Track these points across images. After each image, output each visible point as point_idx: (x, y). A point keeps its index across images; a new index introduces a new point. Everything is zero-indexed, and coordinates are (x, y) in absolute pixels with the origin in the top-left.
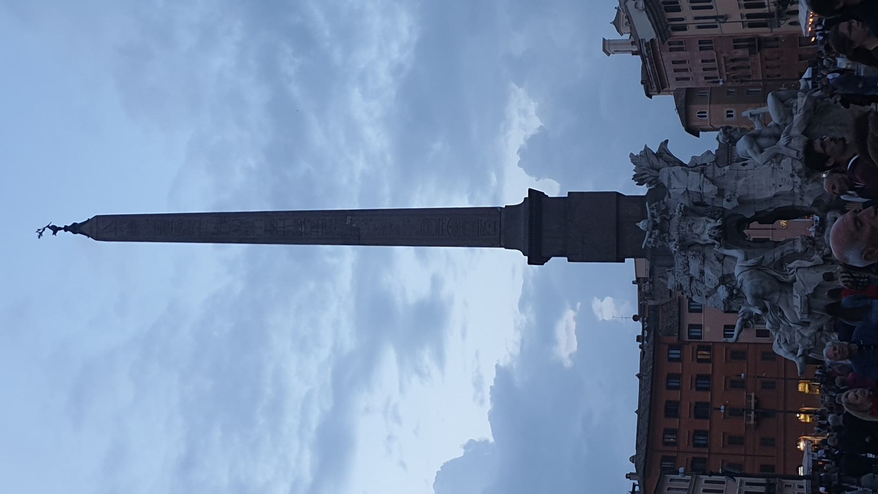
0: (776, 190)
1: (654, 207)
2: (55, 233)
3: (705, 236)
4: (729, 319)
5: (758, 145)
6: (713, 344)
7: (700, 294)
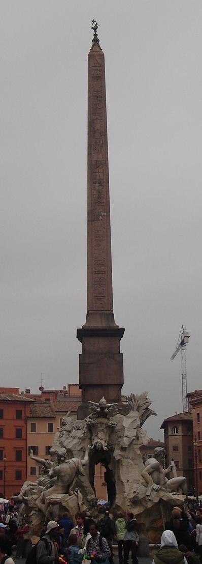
2: (93, 28)
4: (42, 451)
5: (153, 472)
6: (24, 439)
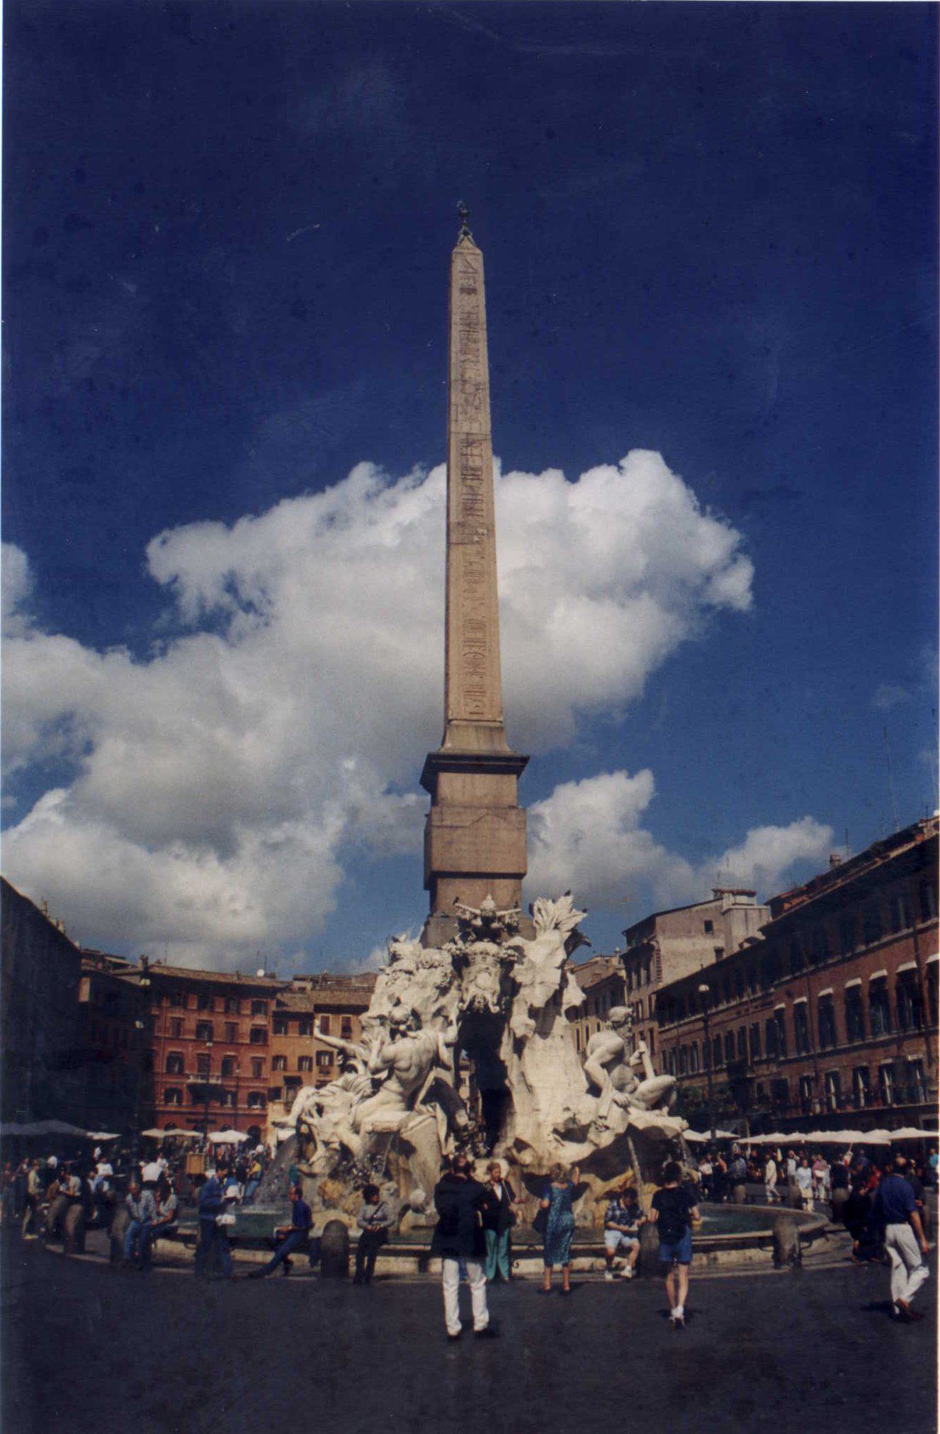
1: (513, 920)
3: (473, 990)
7: (389, 984)
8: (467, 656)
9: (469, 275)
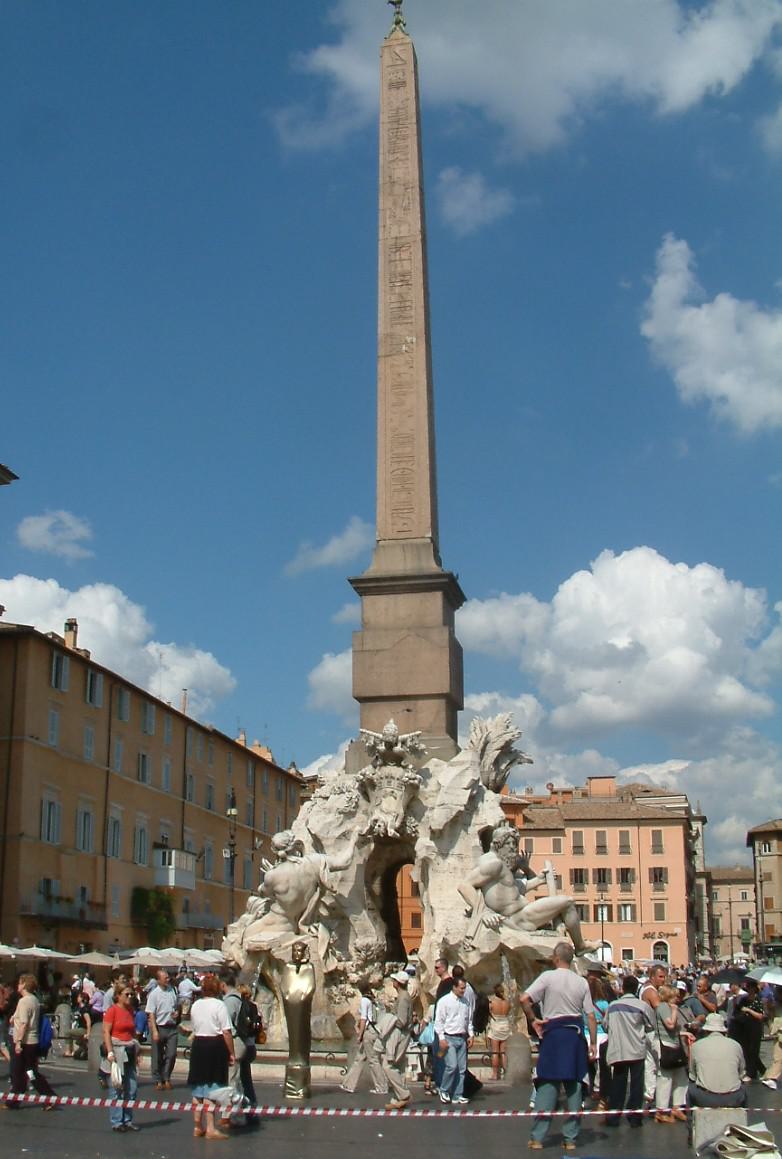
0: (439, 909)
8: (395, 473)
9: (399, 68)
